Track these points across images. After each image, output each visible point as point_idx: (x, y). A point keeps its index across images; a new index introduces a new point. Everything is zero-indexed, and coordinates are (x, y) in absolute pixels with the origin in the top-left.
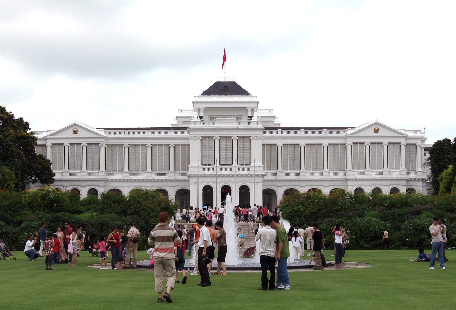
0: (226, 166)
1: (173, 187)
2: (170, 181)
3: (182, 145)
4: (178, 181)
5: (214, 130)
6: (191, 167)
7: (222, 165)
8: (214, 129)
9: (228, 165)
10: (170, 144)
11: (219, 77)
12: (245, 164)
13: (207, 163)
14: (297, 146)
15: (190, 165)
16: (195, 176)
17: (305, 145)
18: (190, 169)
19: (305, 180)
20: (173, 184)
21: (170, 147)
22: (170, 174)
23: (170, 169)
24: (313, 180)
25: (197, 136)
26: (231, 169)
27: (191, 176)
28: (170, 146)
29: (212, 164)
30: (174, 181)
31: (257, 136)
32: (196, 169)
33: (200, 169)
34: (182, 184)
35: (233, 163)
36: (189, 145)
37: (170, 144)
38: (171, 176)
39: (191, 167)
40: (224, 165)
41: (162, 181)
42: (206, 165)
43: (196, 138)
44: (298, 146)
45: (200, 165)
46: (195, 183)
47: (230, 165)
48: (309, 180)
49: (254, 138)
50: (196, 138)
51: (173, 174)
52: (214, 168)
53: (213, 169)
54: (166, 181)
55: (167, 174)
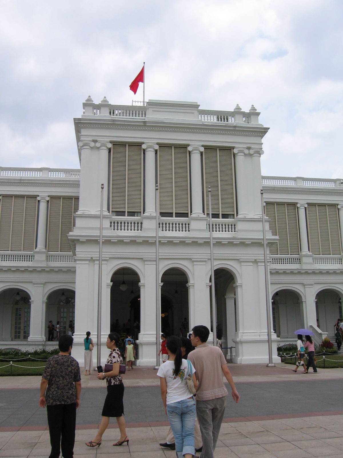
0: (174, 219)
1: (42, 285)
2: (34, 270)
3: (65, 198)
4: (52, 271)
5: (145, 125)
6: (81, 216)
7: (163, 214)
8: (145, 122)
9: (178, 215)
10: (38, 196)
11: (135, 101)
12: (222, 214)
13: (123, 210)
14: (292, 207)
15: (79, 213)
16: (93, 241)
17: (306, 206)
18: (79, 223)
19: (314, 273)
20: (43, 278)
21: (39, 201)
22: (37, 257)
23: (36, 246)
24: (328, 273)
25: (98, 139)
26: (187, 227)
27: (82, 239)
28: (38, 198)
29: (137, 212)
30: (43, 271)
31: (249, 148)
32: (96, 223)
33: (106, 223)
34: (61, 277)
35: (191, 212)
36: (77, 198)
37: (38, 196)
38: (40, 261)
39: (81, 216)
40: (170, 215)
41: (17, 270)
42: (122, 213)
43: (98, 145)
44: (292, 207)
45: (106, 213)
46: (92, 260)
47: (186, 215)
48: (321, 273)
49: (241, 151)
50: (98, 145)
51: (43, 257)
52: (141, 223)
53: (140, 225)
54: (26, 270)
55: (30, 258)
